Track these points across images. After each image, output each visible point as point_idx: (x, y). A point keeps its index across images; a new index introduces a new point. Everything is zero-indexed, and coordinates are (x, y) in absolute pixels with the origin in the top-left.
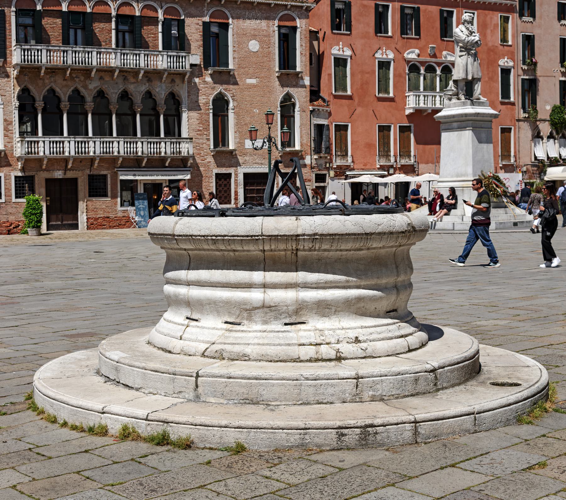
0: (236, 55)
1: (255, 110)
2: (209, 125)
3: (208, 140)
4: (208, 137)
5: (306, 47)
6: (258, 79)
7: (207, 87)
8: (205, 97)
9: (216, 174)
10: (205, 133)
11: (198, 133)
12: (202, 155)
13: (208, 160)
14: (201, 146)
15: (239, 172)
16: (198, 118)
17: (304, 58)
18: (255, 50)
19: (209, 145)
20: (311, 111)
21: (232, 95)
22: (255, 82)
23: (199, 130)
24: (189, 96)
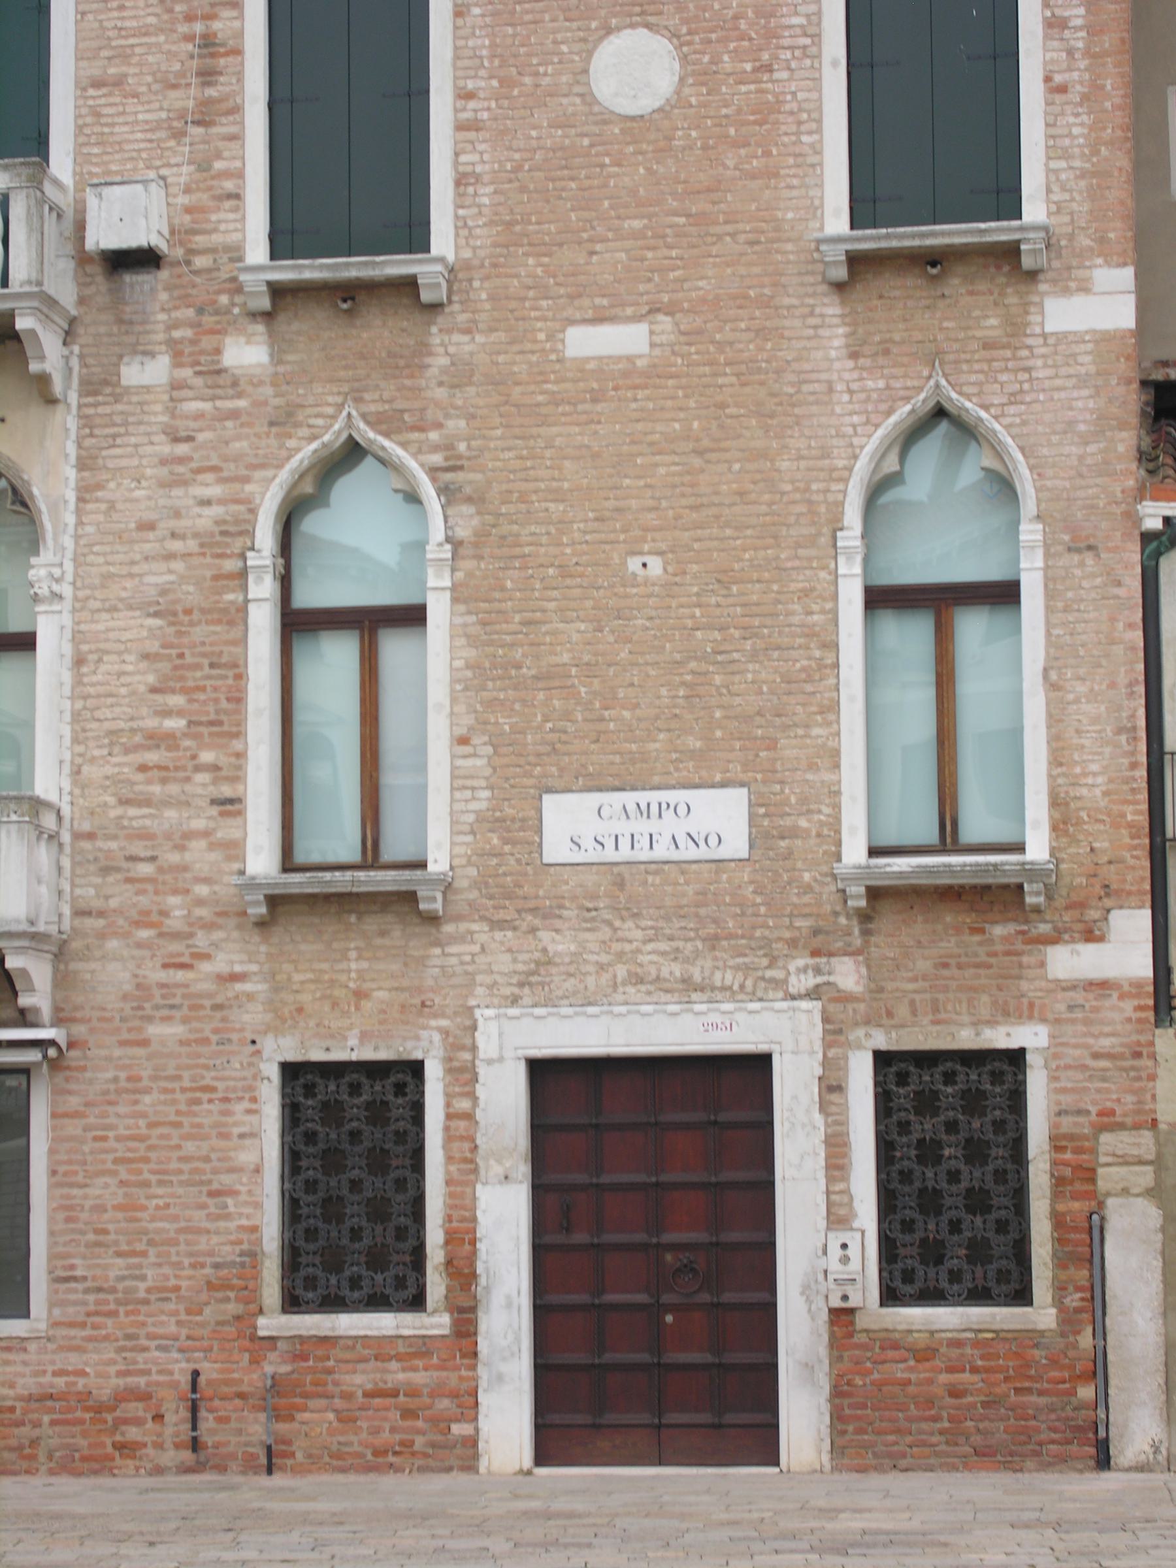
0: (477, 159)
1: (634, 564)
2: (238, 699)
3: (231, 806)
4: (227, 791)
5: (1093, 30)
6: (665, 322)
7: (234, 414)
8: (215, 491)
9: (291, 1071)
10: (207, 757)
11: (152, 757)
12: (175, 922)
13: (221, 964)
14: (174, 858)
15: (487, 1041)
16: (154, 646)
17: (1077, 125)
18: (645, 104)
19: (235, 849)
20: (1147, 537)
21: (437, 459)
22: (645, 349)
23: (156, 739)
24: (85, 493)
